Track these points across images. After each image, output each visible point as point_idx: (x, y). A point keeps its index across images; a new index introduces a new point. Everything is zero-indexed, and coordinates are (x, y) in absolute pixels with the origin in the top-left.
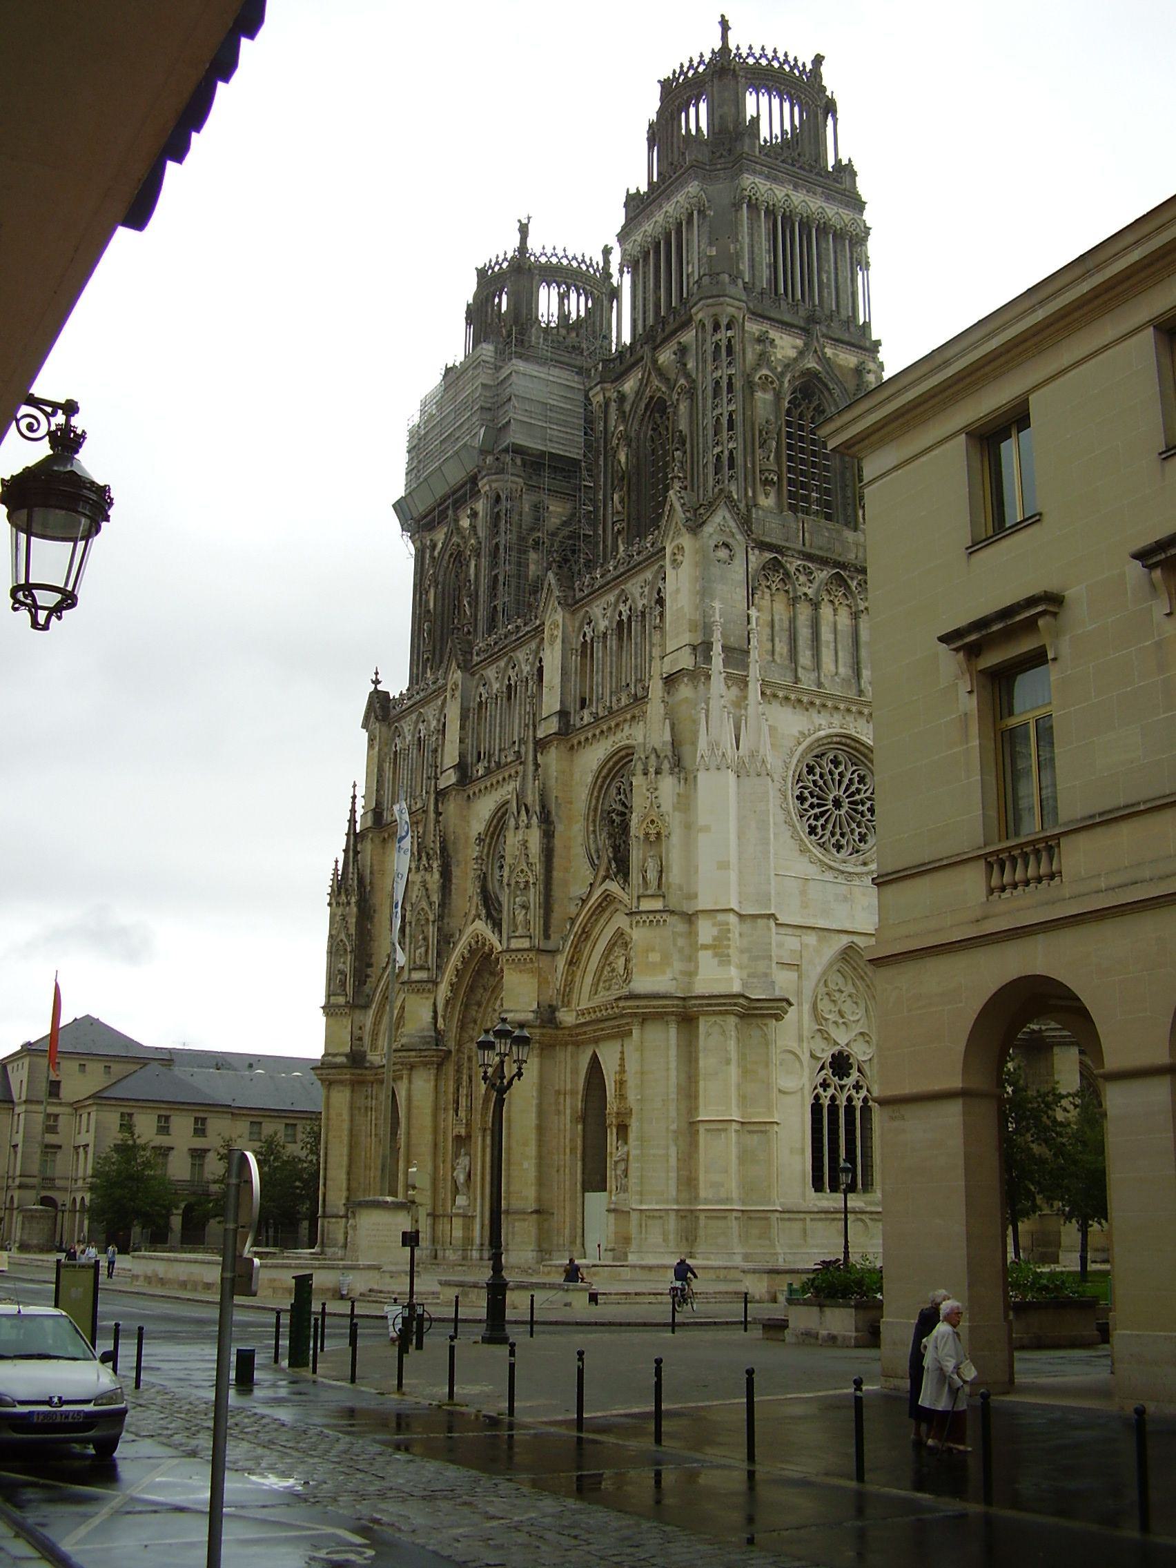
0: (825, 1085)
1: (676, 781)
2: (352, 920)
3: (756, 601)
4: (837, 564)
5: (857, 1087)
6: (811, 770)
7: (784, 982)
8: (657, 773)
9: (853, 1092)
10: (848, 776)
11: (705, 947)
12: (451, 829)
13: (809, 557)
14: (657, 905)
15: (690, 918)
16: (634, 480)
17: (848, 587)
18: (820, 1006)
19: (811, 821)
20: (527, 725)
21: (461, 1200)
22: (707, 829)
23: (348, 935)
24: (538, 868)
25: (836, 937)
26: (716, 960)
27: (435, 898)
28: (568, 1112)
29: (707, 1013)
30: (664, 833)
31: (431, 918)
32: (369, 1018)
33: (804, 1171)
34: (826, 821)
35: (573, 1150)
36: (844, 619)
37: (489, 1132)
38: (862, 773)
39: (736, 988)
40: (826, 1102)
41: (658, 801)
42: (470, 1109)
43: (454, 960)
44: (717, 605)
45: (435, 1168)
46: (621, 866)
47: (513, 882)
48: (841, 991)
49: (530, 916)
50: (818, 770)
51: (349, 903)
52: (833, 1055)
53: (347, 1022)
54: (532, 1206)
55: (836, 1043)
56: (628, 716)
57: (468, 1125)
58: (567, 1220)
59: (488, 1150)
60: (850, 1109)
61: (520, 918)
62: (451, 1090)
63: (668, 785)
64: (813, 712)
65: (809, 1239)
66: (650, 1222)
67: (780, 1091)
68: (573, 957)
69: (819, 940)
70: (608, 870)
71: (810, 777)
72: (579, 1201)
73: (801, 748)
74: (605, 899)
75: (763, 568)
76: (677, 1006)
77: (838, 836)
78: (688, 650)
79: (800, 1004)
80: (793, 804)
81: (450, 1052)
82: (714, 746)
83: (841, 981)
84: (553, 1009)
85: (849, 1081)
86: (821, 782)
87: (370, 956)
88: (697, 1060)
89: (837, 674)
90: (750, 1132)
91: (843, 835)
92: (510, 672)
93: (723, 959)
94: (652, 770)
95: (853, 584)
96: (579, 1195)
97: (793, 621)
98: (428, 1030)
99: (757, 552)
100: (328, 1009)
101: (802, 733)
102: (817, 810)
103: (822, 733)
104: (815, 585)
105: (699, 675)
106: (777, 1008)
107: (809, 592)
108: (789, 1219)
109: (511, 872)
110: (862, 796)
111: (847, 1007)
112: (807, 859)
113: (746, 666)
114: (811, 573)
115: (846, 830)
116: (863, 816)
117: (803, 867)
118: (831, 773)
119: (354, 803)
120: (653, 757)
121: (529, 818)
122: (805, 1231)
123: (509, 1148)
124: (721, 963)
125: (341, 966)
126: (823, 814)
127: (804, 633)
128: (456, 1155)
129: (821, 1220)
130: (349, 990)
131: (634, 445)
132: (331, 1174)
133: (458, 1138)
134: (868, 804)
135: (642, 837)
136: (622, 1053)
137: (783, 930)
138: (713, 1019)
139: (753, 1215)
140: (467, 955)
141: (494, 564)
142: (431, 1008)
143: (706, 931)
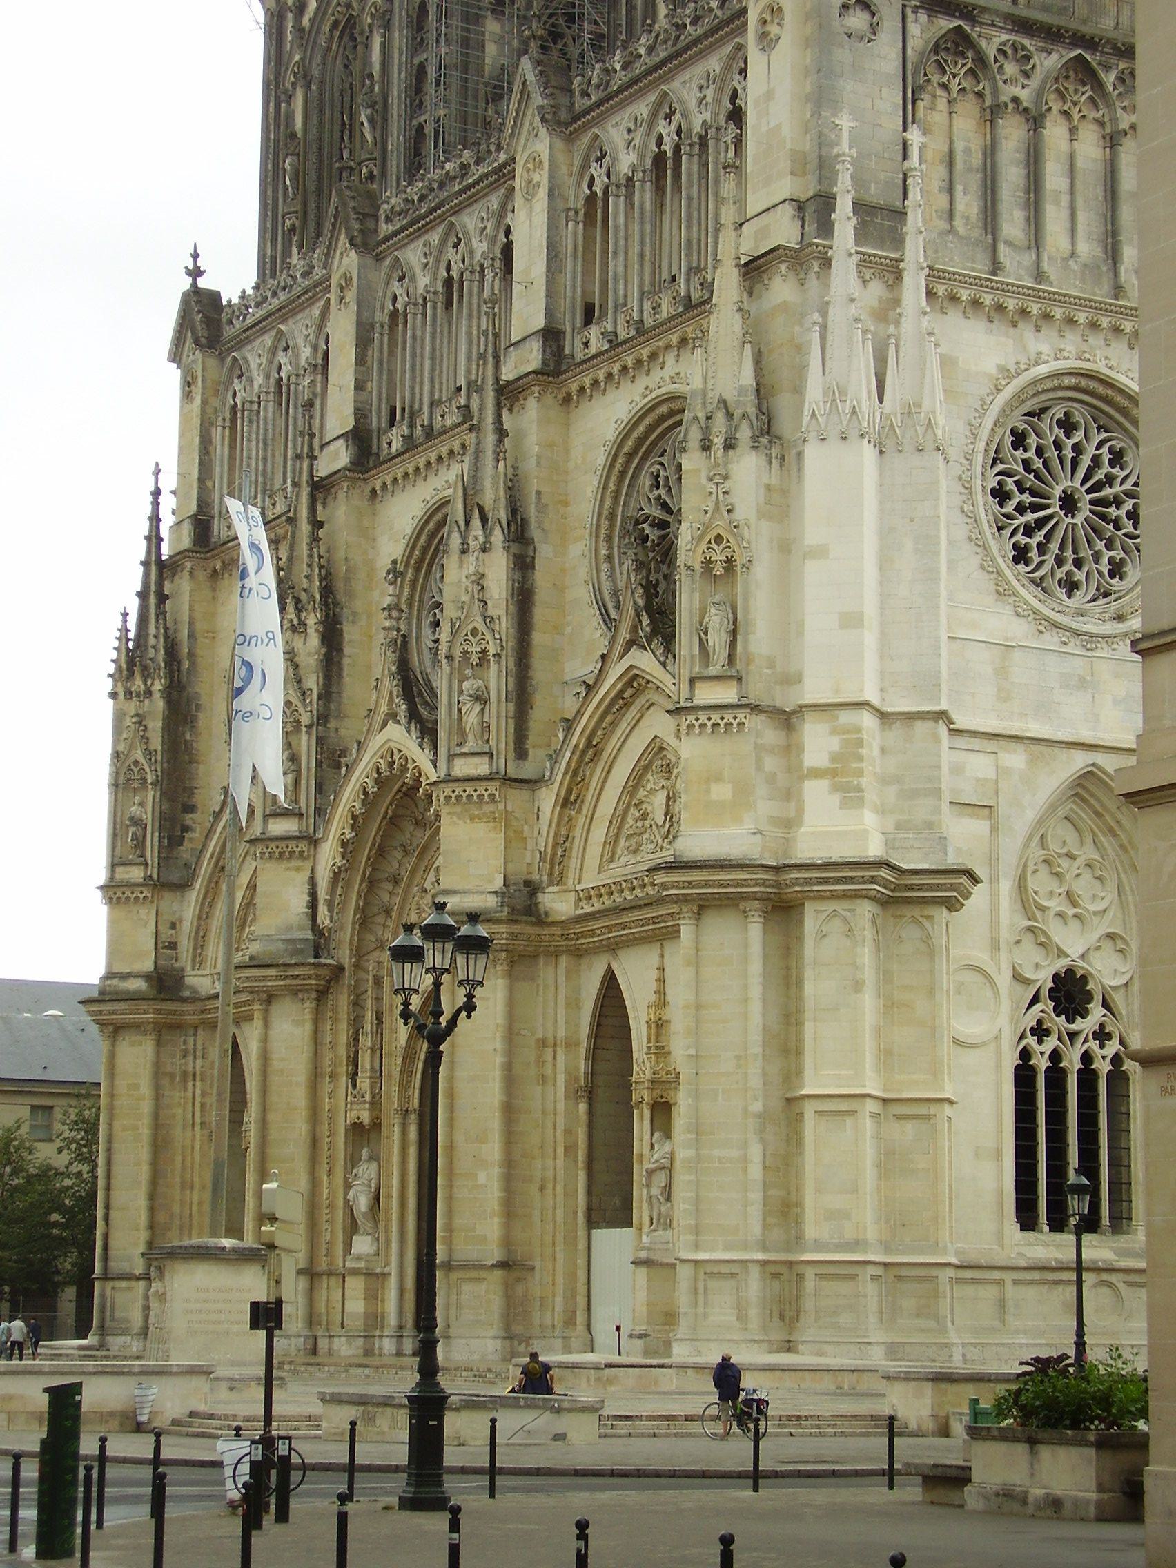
0: (1040, 1031)
1: (762, 461)
2: (156, 725)
3: (920, 113)
4: (1080, 40)
5: (1102, 1035)
6: (1019, 440)
7: (963, 839)
8: (729, 445)
9: (1093, 1045)
10: (1090, 450)
11: (816, 773)
12: (341, 554)
13: (1024, 26)
14: (726, 694)
15: (787, 719)
17: (1099, 85)
18: (1032, 884)
19: (1020, 538)
20: (482, 356)
21: (362, 1244)
22: (820, 552)
23: (149, 753)
24: (505, 626)
25: (1063, 754)
26: (836, 798)
28: (561, 1079)
29: (819, 897)
30: (740, 559)
31: (305, 719)
32: (188, 907)
33: (1000, 1193)
34: (1048, 536)
35: (569, 1150)
36: (1089, 148)
37: (413, 1117)
38: (1118, 445)
39: (874, 850)
40: (1042, 1063)
41: (729, 499)
42: (379, 1074)
43: (348, 798)
44: (845, 122)
45: (314, 1182)
46: (659, 622)
47: (457, 652)
48: (1070, 856)
49: (491, 716)
50: (1033, 440)
51: (149, 693)
52: (1056, 977)
53: (147, 914)
54: (494, 1254)
55: (1061, 953)
56: (675, 339)
57: (376, 1103)
58: (560, 1280)
59: (413, 1151)
60: (1087, 1077)
61: (471, 719)
62: (343, 1039)
63: (748, 469)
64: (1026, 330)
65: (1010, 1319)
66: (712, 1284)
67: (956, 1042)
68: (569, 791)
69: (1033, 761)
70: (634, 629)
71: (1019, 454)
72: (582, 1245)
73: (1001, 399)
74: (629, 684)
75: (936, 49)
76: (764, 883)
77: (1069, 566)
78: (788, 210)
79: (994, 880)
80: (985, 506)
81: (341, 968)
82: (835, 394)
83: (1071, 837)
84: (532, 888)
85: (1087, 1025)
86: (1038, 463)
87: (191, 791)
88: (800, 982)
89: (1073, 254)
90: (899, 1117)
91: (1078, 563)
92: (450, 254)
93: (850, 795)
94: (718, 441)
95: (1109, 79)
96: (582, 1233)
97: (991, 151)
98: (301, 928)
99: (923, 17)
100: (114, 891)
101: (1003, 369)
102: (1030, 517)
103: (1043, 370)
104: (1035, 82)
105: (808, 258)
106: (952, 887)
107: (1025, 95)
108: (974, 1281)
109: (454, 634)
110: (1117, 489)
111: (1083, 886)
112: (1008, 609)
113: (898, 241)
114: (1028, 58)
115: (1086, 553)
116: (1117, 528)
117: (1001, 623)
118: (1058, 445)
119: (156, 504)
120: (720, 417)
121: (487, 533)
122: (1001, 1304)
123: (450, 1148)
124: (844, 804)
125: (135, 810)
126: (1040, 523)
127: (1012, 176)
128: (353, 1161)
129: (1031, 1282)
130: (152, 853)
132: (118, 1197)
133: (357, 1129)
134: (1128, 505)
135: (698, 566)
136: (661, 969)
137: (961, 742)
138: (830, 906)
139: (905, 1272)
140: (372, 788)
141: (417, 44)
142: (306, 888)
143: (818, 744)
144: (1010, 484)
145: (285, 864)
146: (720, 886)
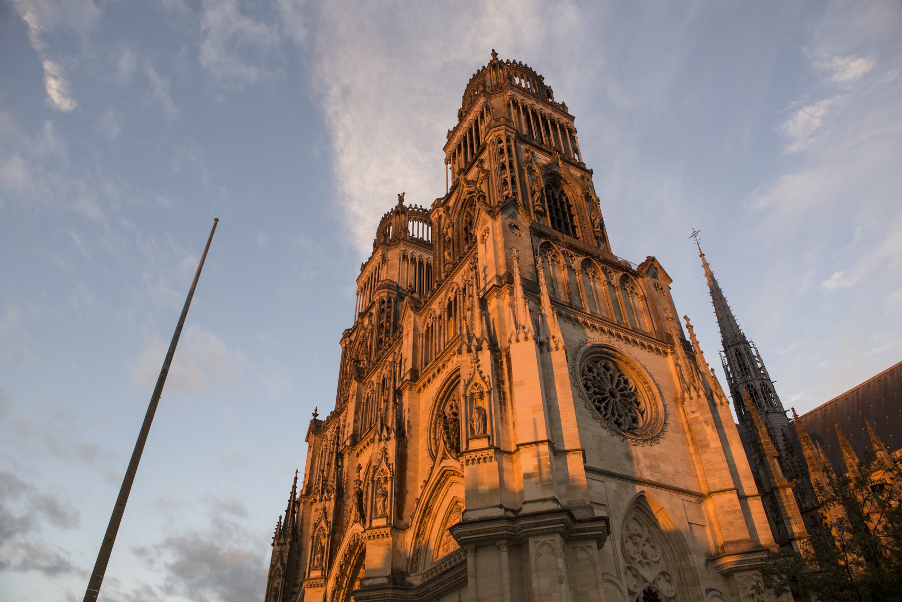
2: (286, 555)
4: (587, 254)
6: (590, 370)
8: (479, 349)
16: (456, 242)
27: (330, 519)
29: (537, 534)
34: (607, 404)
46: (455, 449)
47: (376, 479)
48: (641, 536)
50: (595, 370)
51: (285, 543)
52: (644, 591)
55: (645, 580)
61: (380, 504)
74: (442, 476)
76: (507, 528)
83: (637, 527)
87: (296, 579)
88: (530, 584)
91: (620, 416)
111: (647, 548)
112: (599, 425)
121: (389, 434)
131: (455, 226)
138: (542, 539)
144: (589, 383)
145: (315, 589)
146: (486, 532)
